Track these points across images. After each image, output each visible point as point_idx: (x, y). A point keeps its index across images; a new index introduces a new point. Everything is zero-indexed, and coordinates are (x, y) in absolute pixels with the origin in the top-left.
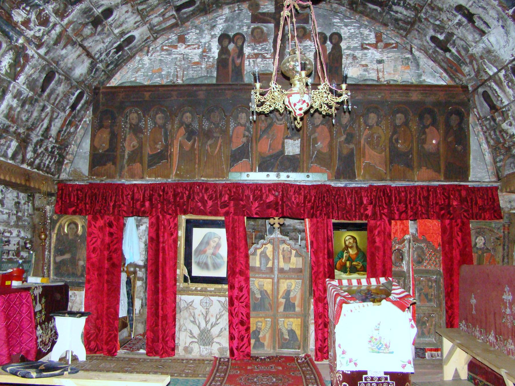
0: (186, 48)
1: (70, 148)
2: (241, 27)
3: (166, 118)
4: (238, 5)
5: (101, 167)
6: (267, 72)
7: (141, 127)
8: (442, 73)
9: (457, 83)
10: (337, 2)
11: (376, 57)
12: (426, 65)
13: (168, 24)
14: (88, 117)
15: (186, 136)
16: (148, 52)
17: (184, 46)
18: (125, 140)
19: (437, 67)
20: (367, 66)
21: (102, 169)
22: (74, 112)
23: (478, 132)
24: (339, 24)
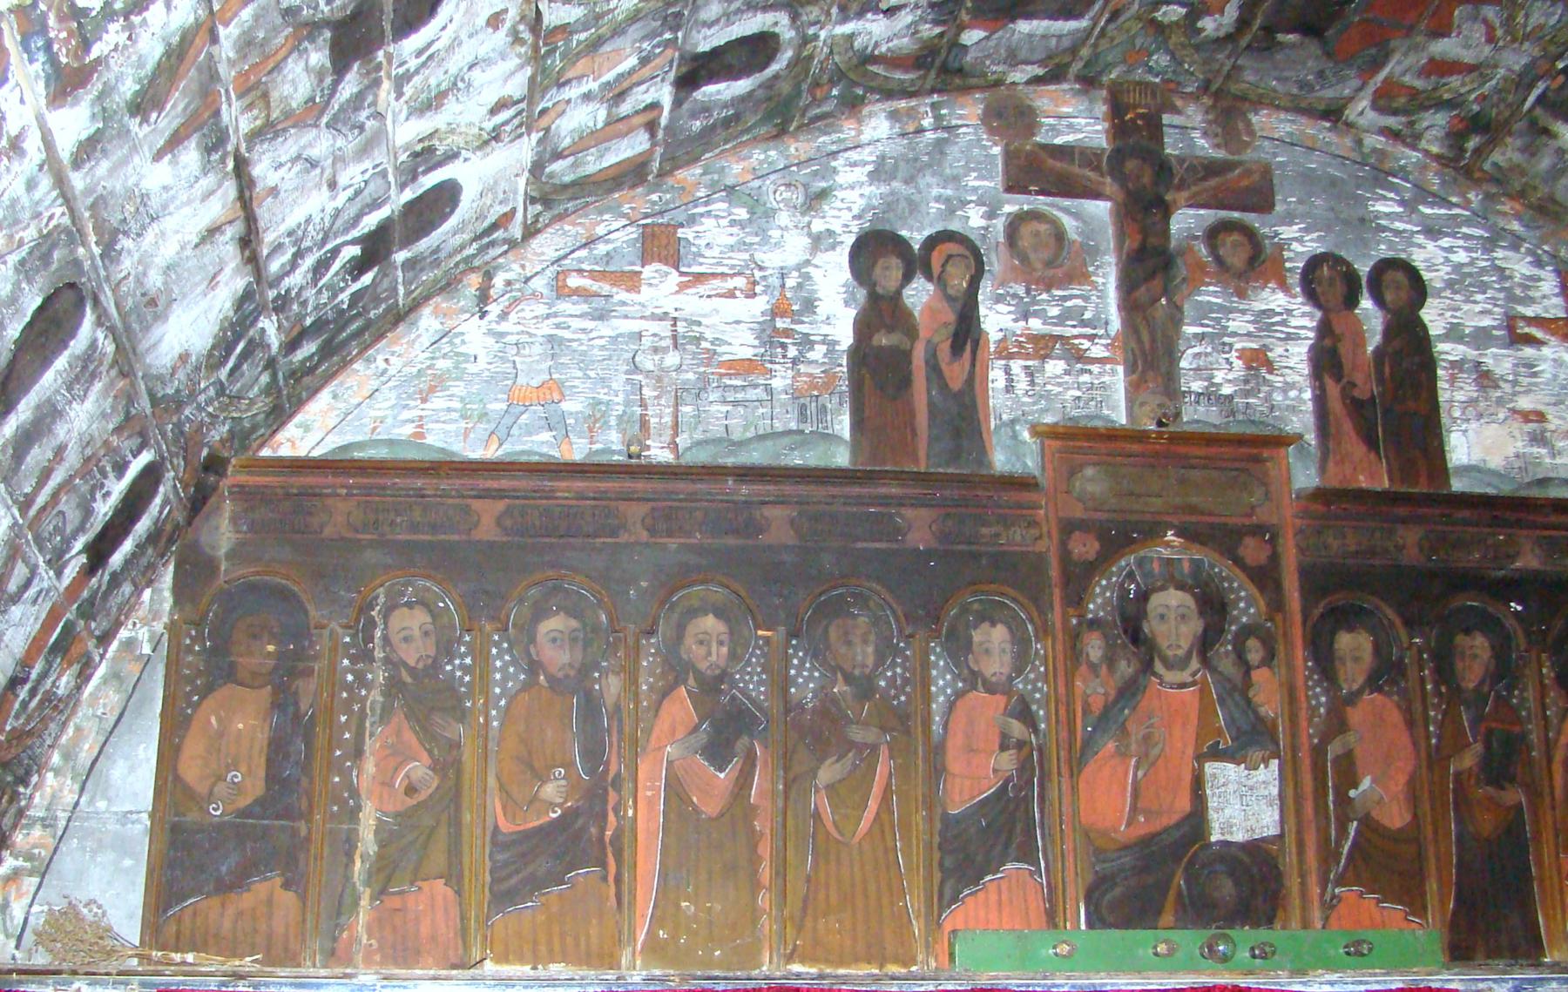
0: (682, 287)
1: (37, 787)
2: (953, 207)
3: (587, 644)
4: (934, 106)
5: (215, 902)
6: (1099, 424)
7: (451, 686)
10: (1392, 122)
13: (611, 159)
14: (146, 622)
15: (702, 737)
16: (484, 297)
17: (674, 278)
18: (358, 753)
20: (1540, 417)
21: (218, 912)
22: (94, 580)
24: (1399, 225)
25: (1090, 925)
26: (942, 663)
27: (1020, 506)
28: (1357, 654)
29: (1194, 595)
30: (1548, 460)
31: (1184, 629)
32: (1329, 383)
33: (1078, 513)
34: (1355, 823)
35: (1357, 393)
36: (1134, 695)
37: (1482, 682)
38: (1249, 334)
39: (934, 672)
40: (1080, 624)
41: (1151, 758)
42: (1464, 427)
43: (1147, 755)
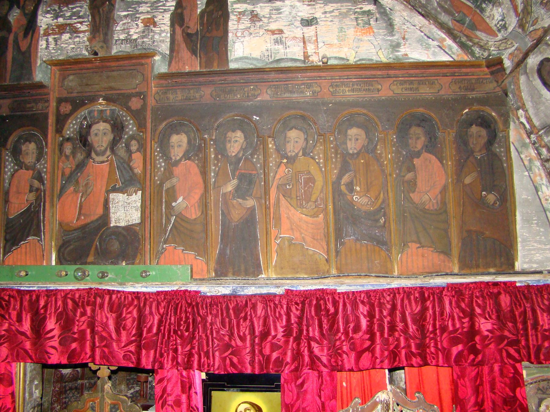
6: (81, 57)
8: (444, 40)
9: (477, 58)
11: (299, 14)
12: (408, 25)
19: (433, 27)
20: (281, 32)
23: (530, 161)
25: (61, 260)
26: (10, 159)
27: (40, 95)
28: (181, 144)
29: (110, 123)
30: (283, 51)
31: (105, 138)
32: (177, 28)
33: (65, 95)
34: (174, 217)
35: (189, 31)
36: (83, 167)
37: (238, 152)
38: (148, 12)
39: (7, 163)
40: (63, 140)
41: (88, 193)
42: (242, 40)
43: (86, 191)
